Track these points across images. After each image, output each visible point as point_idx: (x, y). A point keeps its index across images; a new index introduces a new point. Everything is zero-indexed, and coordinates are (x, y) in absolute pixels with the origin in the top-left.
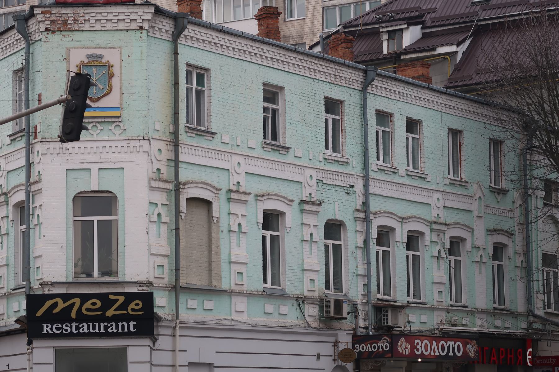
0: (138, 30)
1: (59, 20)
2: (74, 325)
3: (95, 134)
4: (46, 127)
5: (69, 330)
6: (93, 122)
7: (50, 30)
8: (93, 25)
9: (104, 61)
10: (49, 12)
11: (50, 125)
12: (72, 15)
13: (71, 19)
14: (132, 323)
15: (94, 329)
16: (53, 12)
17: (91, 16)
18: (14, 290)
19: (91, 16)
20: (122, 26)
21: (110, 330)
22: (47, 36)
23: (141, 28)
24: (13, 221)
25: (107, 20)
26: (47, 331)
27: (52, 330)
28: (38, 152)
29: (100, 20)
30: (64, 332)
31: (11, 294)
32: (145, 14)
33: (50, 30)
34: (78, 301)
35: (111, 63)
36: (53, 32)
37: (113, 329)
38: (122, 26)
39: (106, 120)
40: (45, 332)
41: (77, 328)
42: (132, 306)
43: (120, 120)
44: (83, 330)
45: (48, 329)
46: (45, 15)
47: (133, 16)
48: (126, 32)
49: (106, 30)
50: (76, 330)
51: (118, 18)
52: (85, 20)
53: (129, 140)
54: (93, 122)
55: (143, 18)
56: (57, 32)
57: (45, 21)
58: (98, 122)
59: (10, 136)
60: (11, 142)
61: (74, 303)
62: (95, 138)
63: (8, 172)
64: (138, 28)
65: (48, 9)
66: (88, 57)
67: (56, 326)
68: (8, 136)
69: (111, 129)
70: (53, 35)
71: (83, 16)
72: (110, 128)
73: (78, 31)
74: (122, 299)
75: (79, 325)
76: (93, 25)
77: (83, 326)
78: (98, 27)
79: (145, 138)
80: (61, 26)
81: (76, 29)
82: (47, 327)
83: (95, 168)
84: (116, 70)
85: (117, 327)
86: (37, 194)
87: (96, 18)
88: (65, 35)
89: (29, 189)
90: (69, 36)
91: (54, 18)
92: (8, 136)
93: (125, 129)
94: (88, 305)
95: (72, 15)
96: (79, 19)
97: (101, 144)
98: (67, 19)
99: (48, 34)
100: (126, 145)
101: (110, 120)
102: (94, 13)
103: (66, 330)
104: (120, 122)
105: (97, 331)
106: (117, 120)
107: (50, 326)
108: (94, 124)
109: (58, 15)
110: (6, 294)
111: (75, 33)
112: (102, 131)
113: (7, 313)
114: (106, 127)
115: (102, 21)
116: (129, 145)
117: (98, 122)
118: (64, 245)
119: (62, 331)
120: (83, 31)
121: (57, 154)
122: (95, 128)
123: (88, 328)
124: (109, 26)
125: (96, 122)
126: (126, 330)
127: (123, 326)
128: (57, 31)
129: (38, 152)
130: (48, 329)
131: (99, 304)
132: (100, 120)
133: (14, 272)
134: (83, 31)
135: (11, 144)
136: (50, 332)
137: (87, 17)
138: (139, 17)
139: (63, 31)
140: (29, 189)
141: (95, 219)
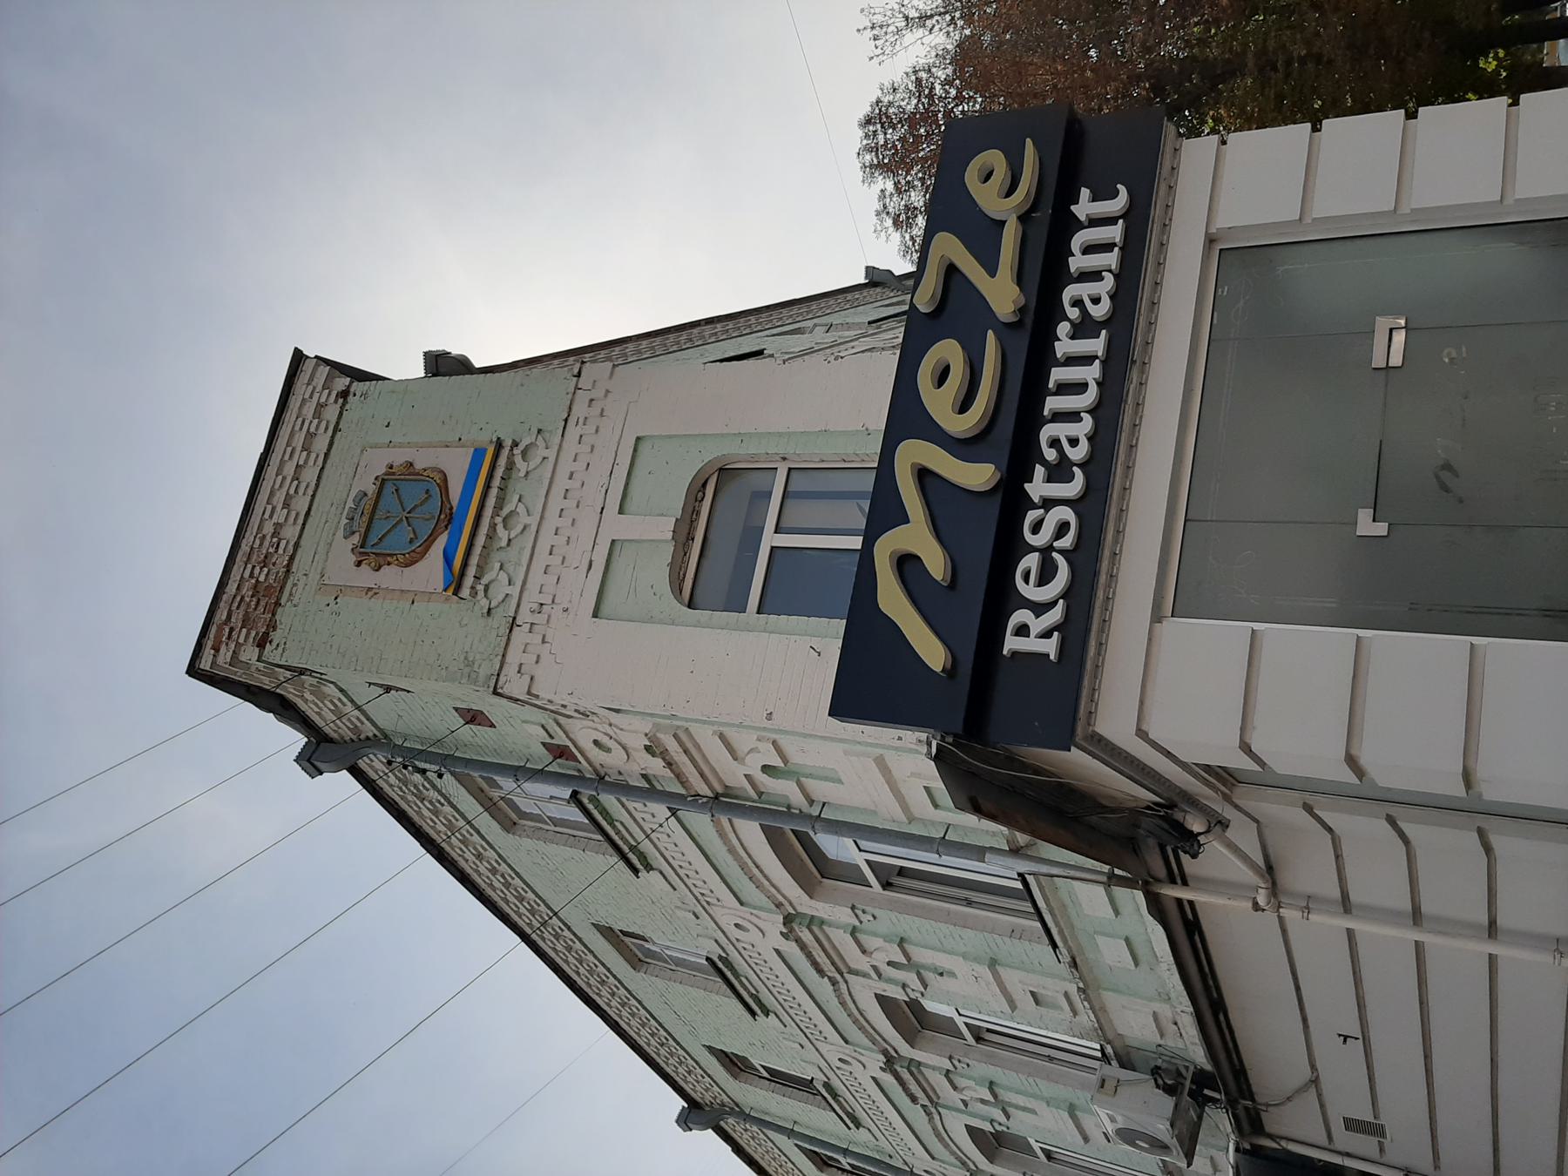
0: (343, 405)
1: (249, 605)
2: (1038, 487)
3: (524, 519)
4: (467, 670)
5: (1066, 514)
6: (493, 527)
7: (266, 634)
8: (293, 514)
9: (371, 489)
10: (220, 629)
11: (466, 658)
12: (249, 566)
13: (257, 570)
14: (1084, 207)
15: (1080, 388)
16: (224, 617)
17: (271, 517)
18: (1054, 946)
19: (271, 517)
20: (321, 444)
21: (1099, 312)
22: (274, 646)
23: (344, 394)
24: (853, 908)
25: (296, 478)
26: (1047, 634)
27: (1051, 605)
28: (596, 742)
29: (288, 493)
30: (1067, 542)
31: (1074, 964)
32: (314, 383)
33: (266, 634)
34: (914, 453)
35: (381, 470)
36: (272, 626)
37: (1097, 297)
38: (321, 444)
39: (496, 482)
40: (1050, 647)
41: (1059, 472)
42: (990, 199)
43: (508, 443)
44: (1074, 442)
45: (1038, 624)
46: (224, 639)
47: (309, 410)
48: (339, 434)
49: (317, 485)
50: (1070, 478)
51: (299, 449)
52: (272, 537)
53: (566, 421)
54: (493, 527)
55: (319, 388)
56: (277, 617)
57: (238, 645)
58: (499, 507)
59: (636, 871)
60: (656, 869)
61: (924, 475)
62: (533, 521)
63: (742, 904)
64: (341, 401)
65: (213, 630)
66: (349, 533)
67: (1026, 580)
68: (638, 877)
69: (527, 473)
70: (279, 626)
71: (264, 536)
72: (522, 474)
73: (292, 558)
74: (950, 247)
75: (1044, 463)
76: (293, 514)
77: (1055, 443)
78: (301, 504)
79: (576, 371)
80: (262, 603)
81: (286, 562)
82: (1022, 630)
83: (617, 527)
84: (399, 457)
85: (1094, 276)
86: (720, 780)
87: (280, 506)
88: (291, 594)
89: (705, 800)
90: (295, 585)
91: (237, 620)
92: (638, 877)
93: (539, 431)
94: (939, 403)
95: (249, 566)
96: (264, 552)
97: (556, 502)
98: (253, 581)
99: (270, 642)
100: (579, 430)
101: (499, 472)
102: (265, 508)
103: (1062, 529)
104: (515, 444)
105: (1092, 373)
106: (505, 453)
107: (1021, 616)
108: (499, 520)
109: (236, 604)
110: (1081, 985)
111: (294, 569)
112: (522, 500)
113: (1151, 1000)
114: (517, 487)
115: (292, 491)
116: (581, 421)
117: (499, 507)
118: (815, 642)
119: (1061, 552)
120: (297, 545)
121: (544, 642)
122: (511, 522)
123: (1073, 416)
124: (310, 475)
125: (496, 513)
126: (1115, 233)
127: (1088, 250)
128: (273, 615)
129: (596, 742)
130: (1038, 624)
131: (948, 351)
132: (491, 501)
133: (1007, 940)
134: (297, 545)
135: (661, 873)
136: (1055, 615)
137: (268, 528)
138: (316, 396)
139: (279, 599)
140: (705, 800)
141: (770, 539)
